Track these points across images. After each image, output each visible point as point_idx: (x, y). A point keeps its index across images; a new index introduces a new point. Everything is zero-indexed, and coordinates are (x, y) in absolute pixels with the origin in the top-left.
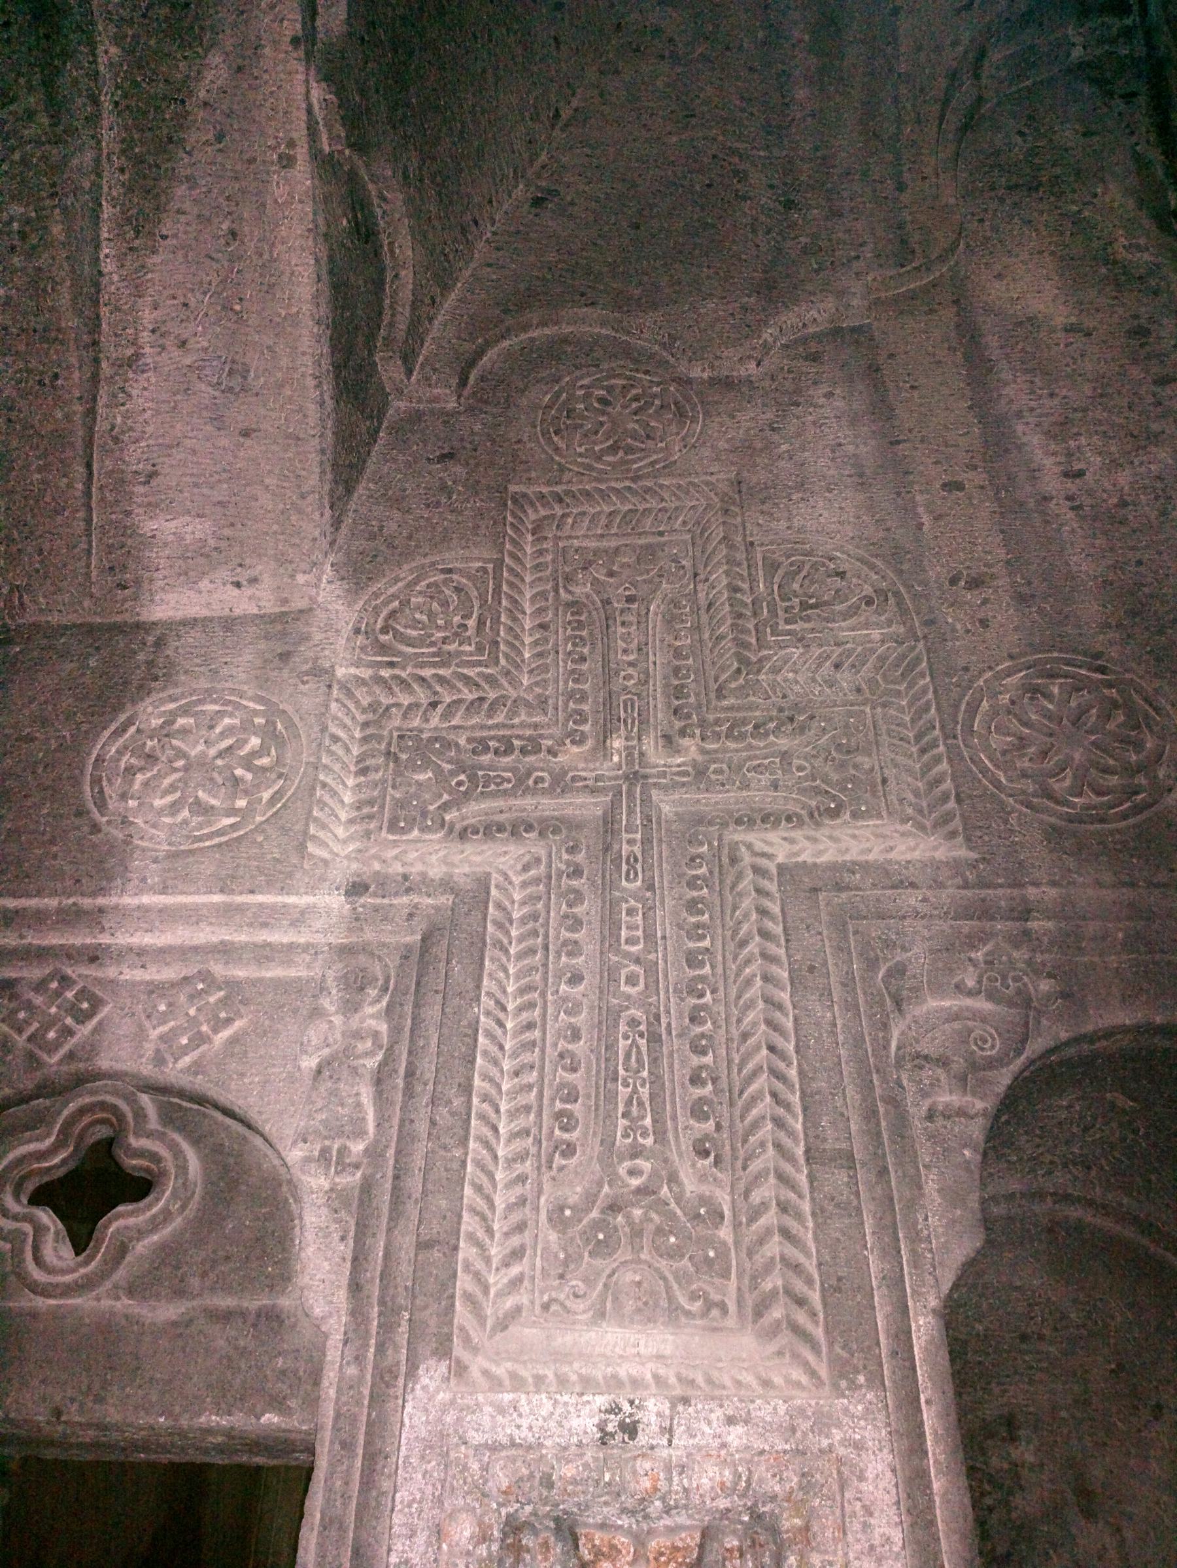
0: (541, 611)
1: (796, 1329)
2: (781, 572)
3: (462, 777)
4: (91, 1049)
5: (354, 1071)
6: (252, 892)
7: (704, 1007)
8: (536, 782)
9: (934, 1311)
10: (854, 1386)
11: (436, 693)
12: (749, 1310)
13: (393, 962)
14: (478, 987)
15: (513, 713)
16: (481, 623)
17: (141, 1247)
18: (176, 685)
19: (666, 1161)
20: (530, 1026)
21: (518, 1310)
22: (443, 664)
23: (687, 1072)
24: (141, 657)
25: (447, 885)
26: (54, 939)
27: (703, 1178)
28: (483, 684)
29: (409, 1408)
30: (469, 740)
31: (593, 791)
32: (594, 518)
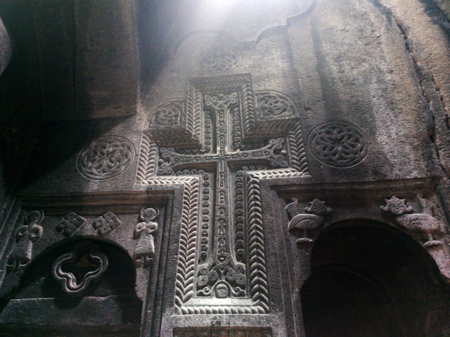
9: (297, 293)
14: (181, 214)
19: (230, 257)
26: (70, 204)
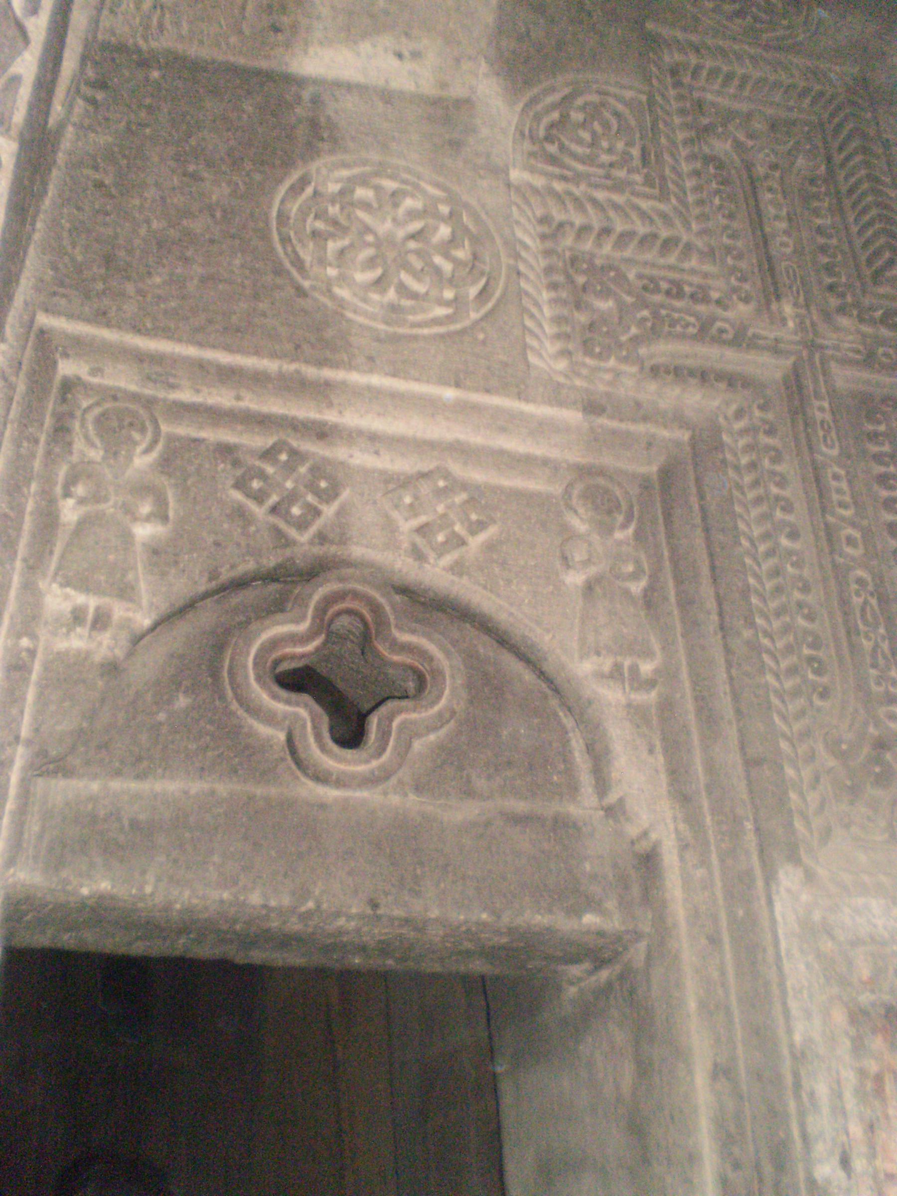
5: (627, 592)
6: (487, 391)
11: (608, 219)
13: (634, 491)
18: (346, 151)
26: (275, 406)
28: (656, 218)
29: (778, 907)
30: (640, 276)
32: (729, 77)
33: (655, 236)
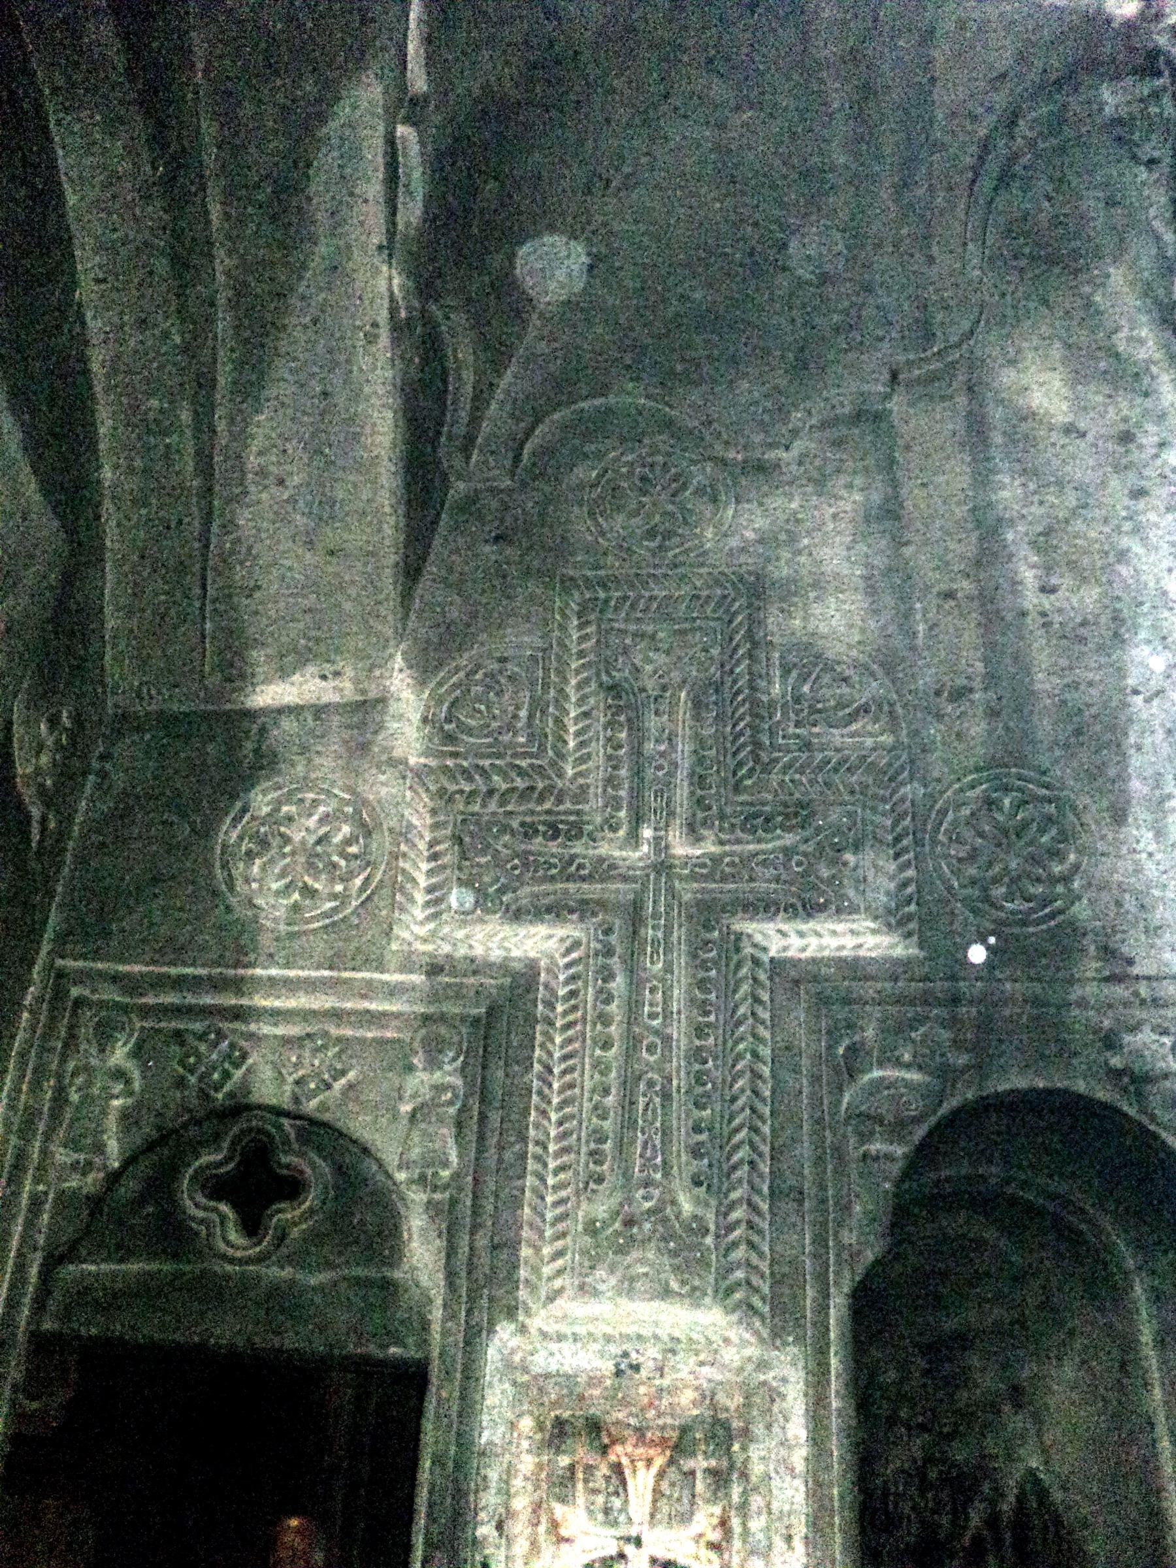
0: (582, 700)
1: (751, 1307)
2: (794, 674)
3: (516, 861)
4: (245, 1088)
7: (707, 1073)
8: (577, 870)
10: (785, 1344)
12: (720, 1295)
15: (560, 801)
16: (531, 717)
17: (295, 1233)
18: (279, 773)
20: (571, 1086)
21: (563, 1289)
22: (499, 756)
23: (690, 1123)
24: (249, 745)
25: (504, 967)
26: (208, 1000)
27: (697, 1201)
30: (523, 824)
31: (625, 879)
33: (532, 788)
